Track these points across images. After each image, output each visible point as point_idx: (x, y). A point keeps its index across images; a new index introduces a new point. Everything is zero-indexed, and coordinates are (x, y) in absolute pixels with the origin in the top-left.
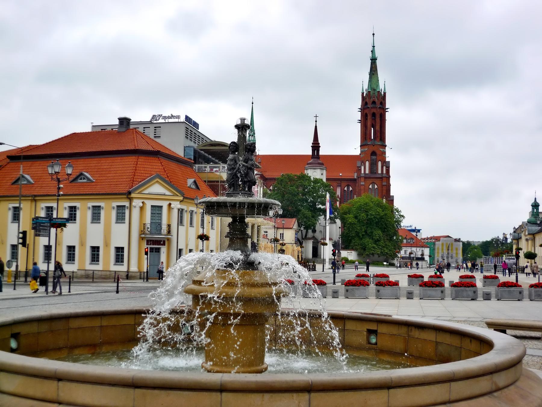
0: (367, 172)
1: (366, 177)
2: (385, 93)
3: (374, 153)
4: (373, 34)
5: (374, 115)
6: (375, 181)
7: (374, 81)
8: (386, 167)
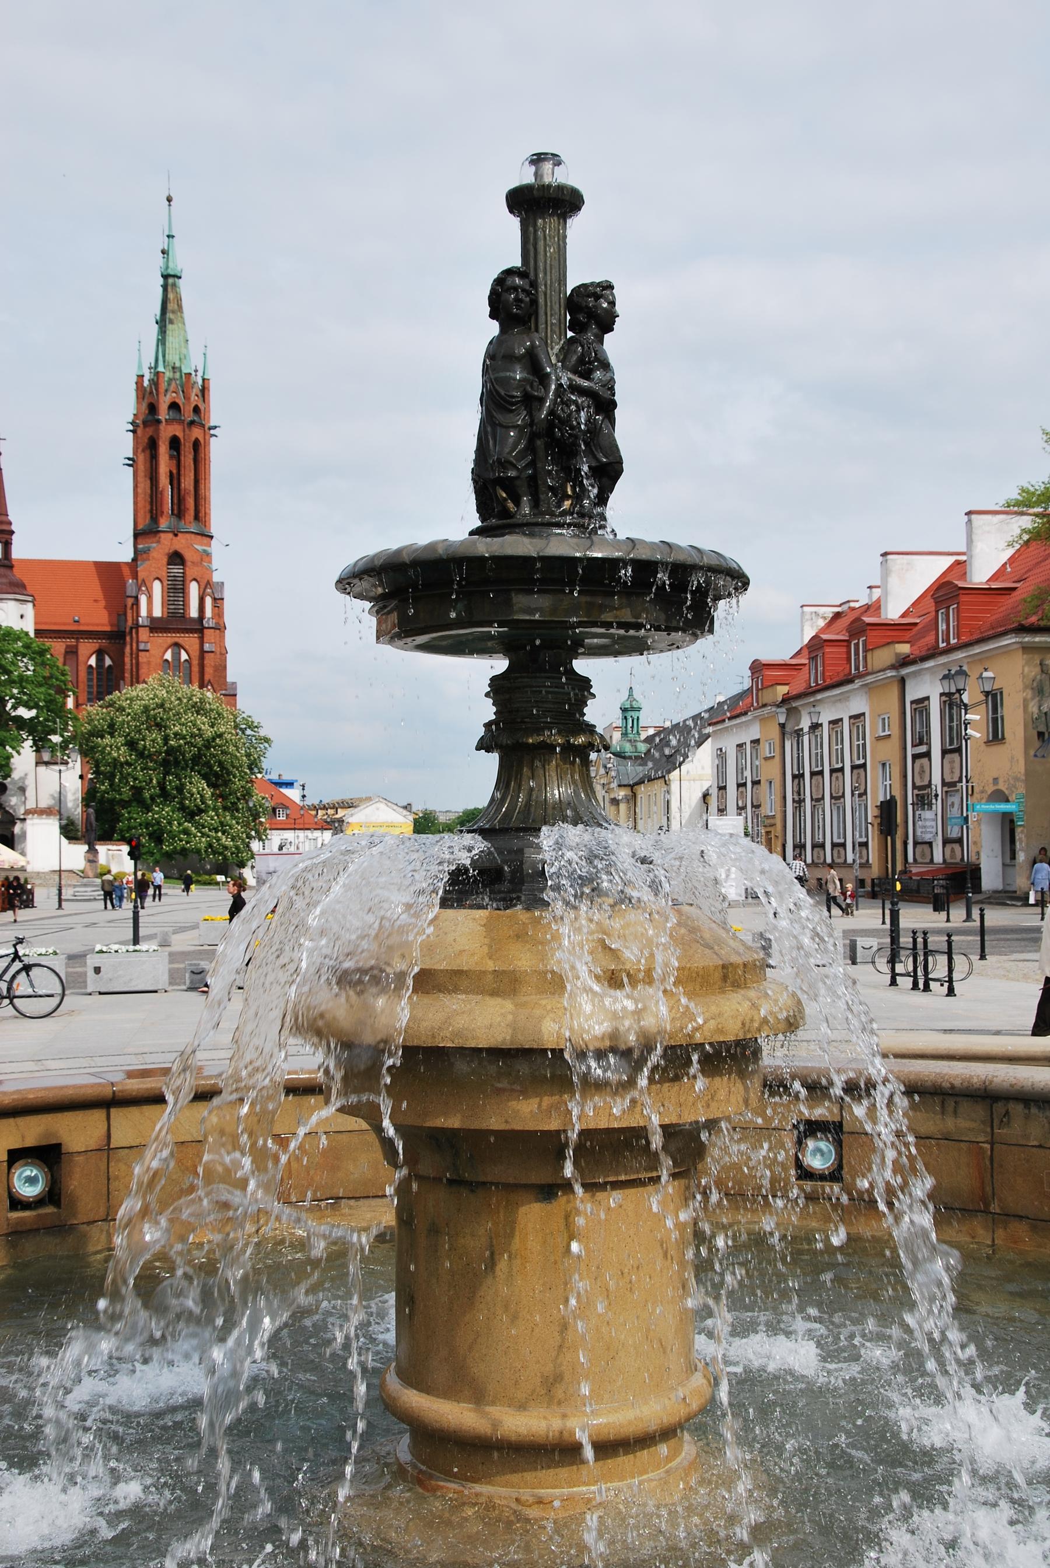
0: (157, 612)
1: (157, 626)
3: (176, 558)
4: (169, 200)
5: (175, 443)
6: (180, 641)
7: (172, 340)
8: (215, 600)
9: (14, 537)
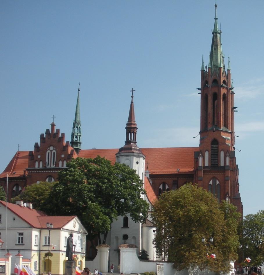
0: (207, 164)
1: (206, 170)
2: (229, 70)
9: (137, 130)
